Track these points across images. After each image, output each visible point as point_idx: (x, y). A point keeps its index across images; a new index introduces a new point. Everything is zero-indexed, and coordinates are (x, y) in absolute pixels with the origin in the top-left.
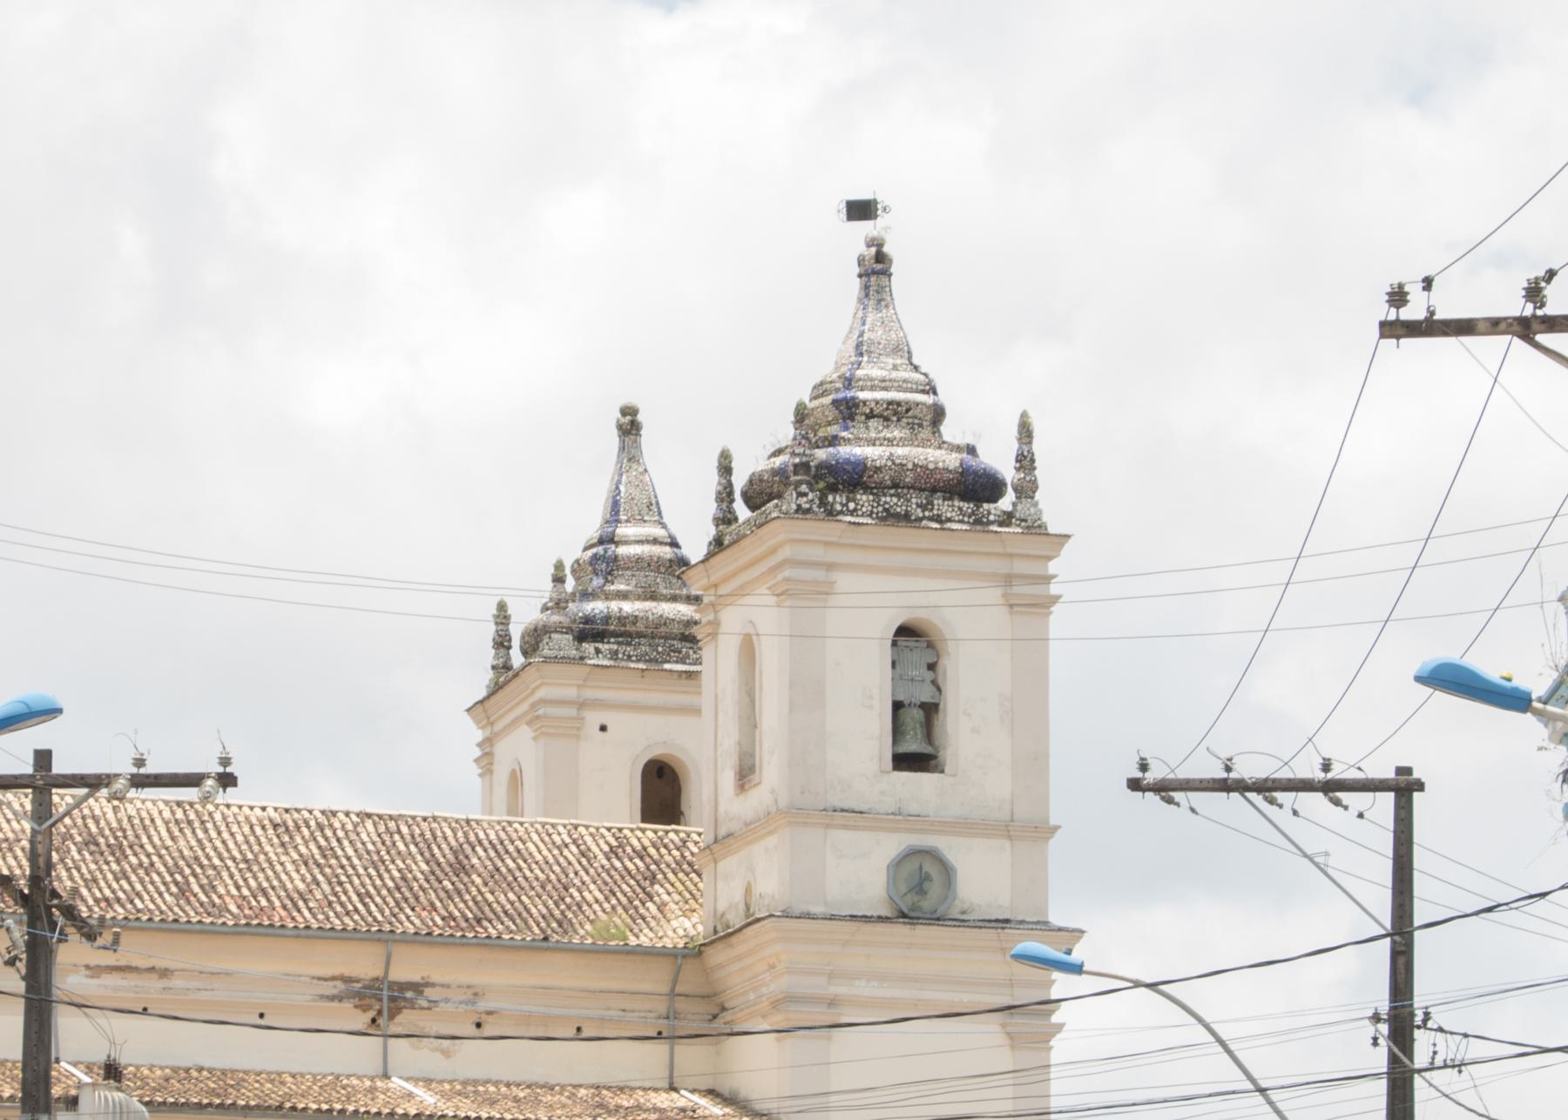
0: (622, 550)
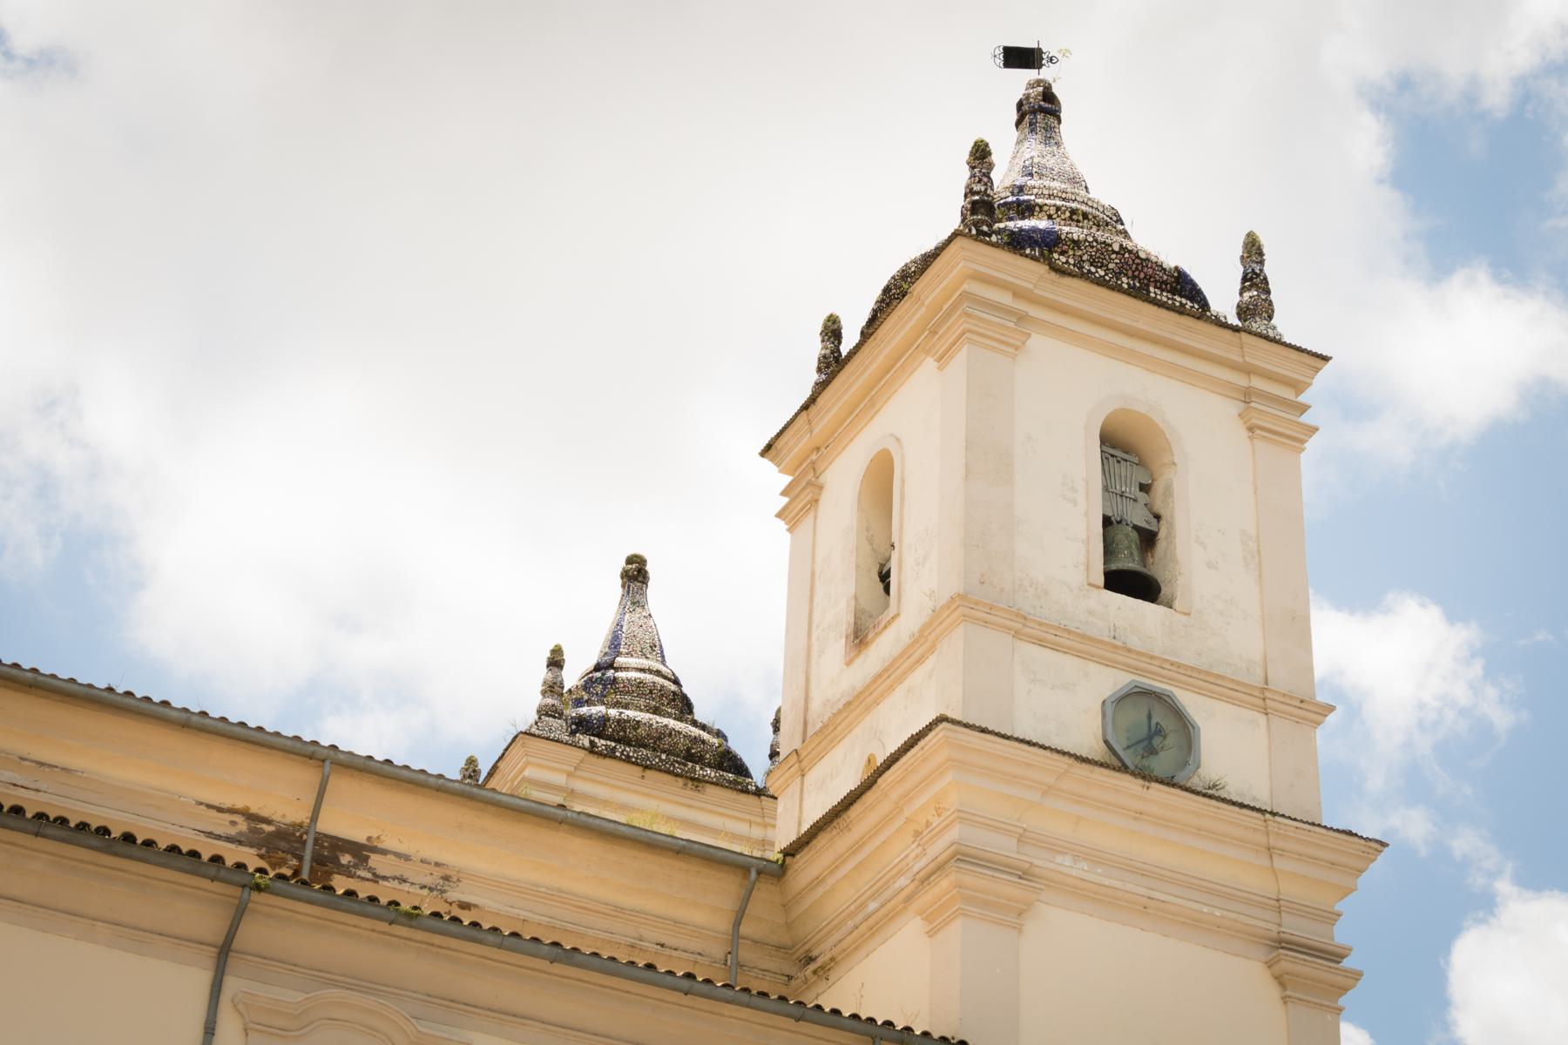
0: (620, 675)
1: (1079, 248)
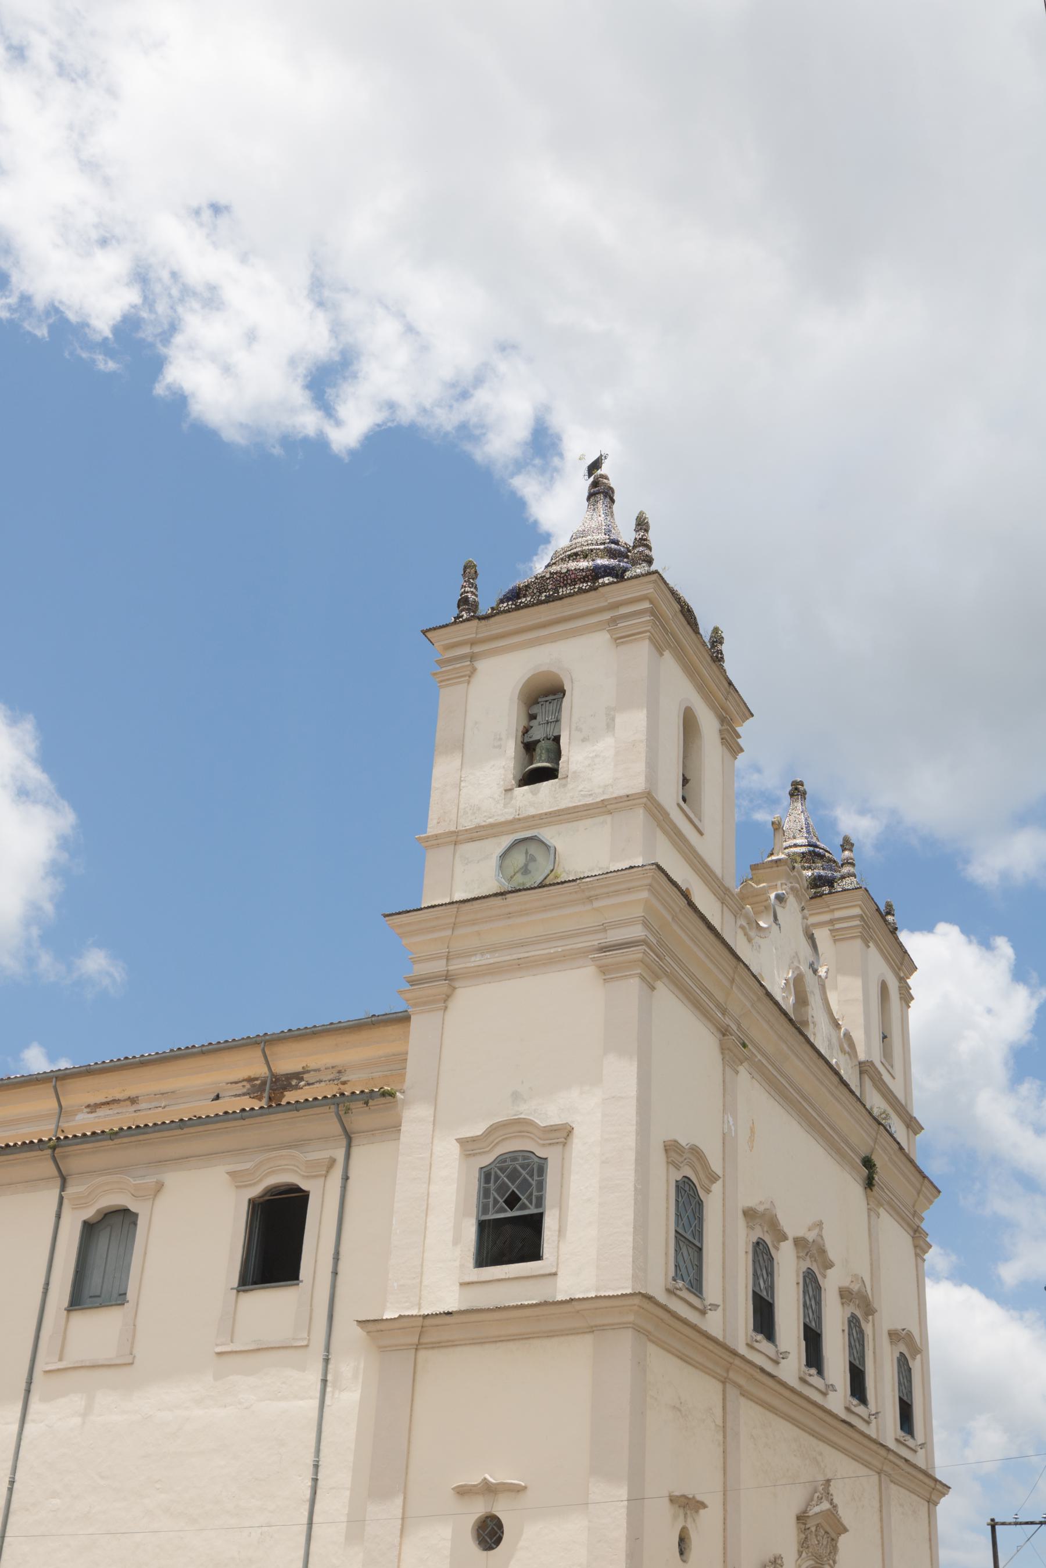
1: (530, 588)
